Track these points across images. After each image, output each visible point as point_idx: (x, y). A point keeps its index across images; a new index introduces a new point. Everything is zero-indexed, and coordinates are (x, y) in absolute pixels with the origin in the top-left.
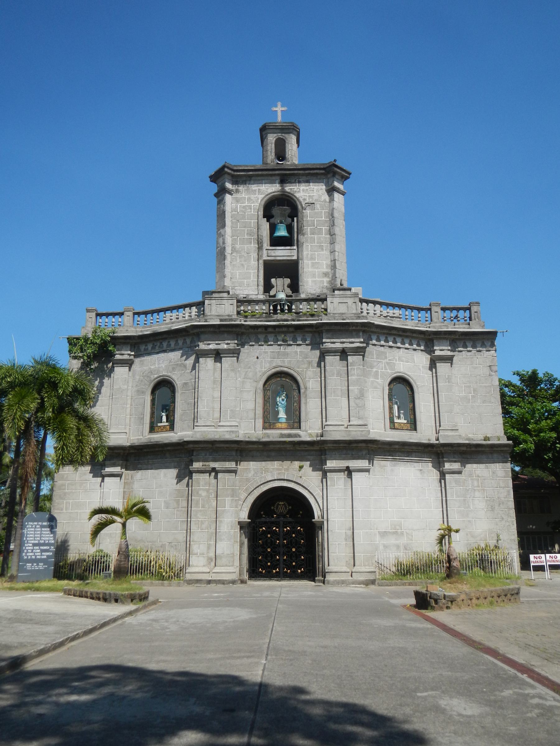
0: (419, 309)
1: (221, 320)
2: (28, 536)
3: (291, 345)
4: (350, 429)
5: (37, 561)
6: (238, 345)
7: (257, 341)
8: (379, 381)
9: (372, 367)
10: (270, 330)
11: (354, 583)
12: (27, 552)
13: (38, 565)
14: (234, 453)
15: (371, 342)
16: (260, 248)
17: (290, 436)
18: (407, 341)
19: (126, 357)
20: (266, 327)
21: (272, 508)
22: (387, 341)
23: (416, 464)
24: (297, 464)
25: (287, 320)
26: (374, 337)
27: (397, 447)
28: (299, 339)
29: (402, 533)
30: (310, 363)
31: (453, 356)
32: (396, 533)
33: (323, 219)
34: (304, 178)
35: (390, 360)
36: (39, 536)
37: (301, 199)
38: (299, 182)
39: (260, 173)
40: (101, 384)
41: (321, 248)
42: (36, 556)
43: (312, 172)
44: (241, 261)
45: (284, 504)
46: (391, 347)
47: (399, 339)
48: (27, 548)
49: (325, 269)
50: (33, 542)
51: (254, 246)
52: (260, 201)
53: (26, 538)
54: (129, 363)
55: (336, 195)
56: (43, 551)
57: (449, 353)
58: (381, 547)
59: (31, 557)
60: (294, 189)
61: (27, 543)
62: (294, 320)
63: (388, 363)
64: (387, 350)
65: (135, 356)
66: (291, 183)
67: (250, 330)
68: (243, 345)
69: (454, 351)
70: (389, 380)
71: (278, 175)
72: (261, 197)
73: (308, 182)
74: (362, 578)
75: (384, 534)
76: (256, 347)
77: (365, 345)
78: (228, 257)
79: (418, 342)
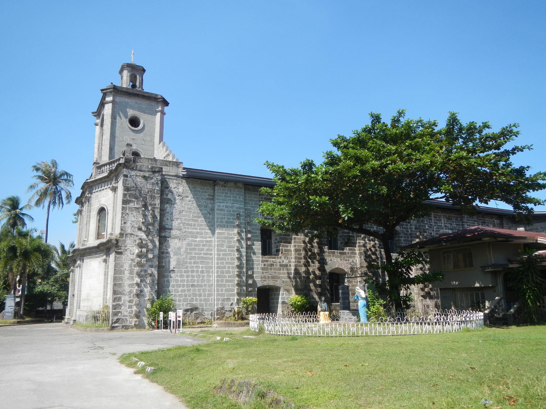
15: (93, 192)
46: (100, 191)
47: (103, 185)
63: (98, 201)
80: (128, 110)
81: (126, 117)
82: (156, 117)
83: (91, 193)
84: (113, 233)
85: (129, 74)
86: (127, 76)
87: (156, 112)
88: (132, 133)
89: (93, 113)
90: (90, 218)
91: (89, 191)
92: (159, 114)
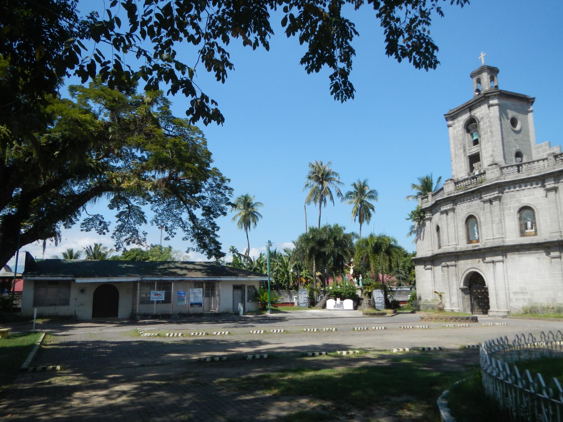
0: (543, 160)
1: (448, 195)
3: (472, 201)
4: (495, 240)
5: (379, 303)
6: (453, 205)
7: (460, 202)
8: (512, 211)
9: (507, 205)
10: (463, 196)
11: (499, 316)
14: (454, 257)
15: (505, 191)
16: (464, 151)
17: (476, 246)
18: (529, 184)
19: (429, 217)
20: (461, 195)
22: (515, 188)
23: (534, 255)
24: (477, 260)
25: (471, 188)
26: (507, 188)
27: (518, 247)
28: (475, 197)
29: (527, 293)
30: (481, 208)
32: (523, 293)
34: (478, 104)
37: (478, 117)
38: (477, 108)
39: (459, 111)
40: (424, 229)
41: (488, 141)
43: (479, 100)
47: (523, 185)
49: (491, 153)
51: (462, 150)
54: (430, 219)
55: (491, 108)
56: (380, 300)
57: (553, 185)
58: (514, 300)
62: (474, 187)
63: (517, 200)
64: (516, 193)
65: (432, 215)
66: (473, 109)
67: (456, 198)
68: (456, 205)
69: (558, 183)
70: (517, 209)
71: (467, 108)
73: (480, 106)
74: (502, 314)
75: (515, 293)
76: (461, 205)
77: (500, 195)
78: (453, 160)
79: (537, 182)
80: (508, 111)
81: (508, 119)
82: (527, 118)
83: (503, 193)
84: (561, 230)
85: (489, 76)
86: (488, 78)
87: (527, 112)
88: (514, 134)
89: (445, 115)
90: (504, 216)
91: (499, 191)
92: (530, 115)
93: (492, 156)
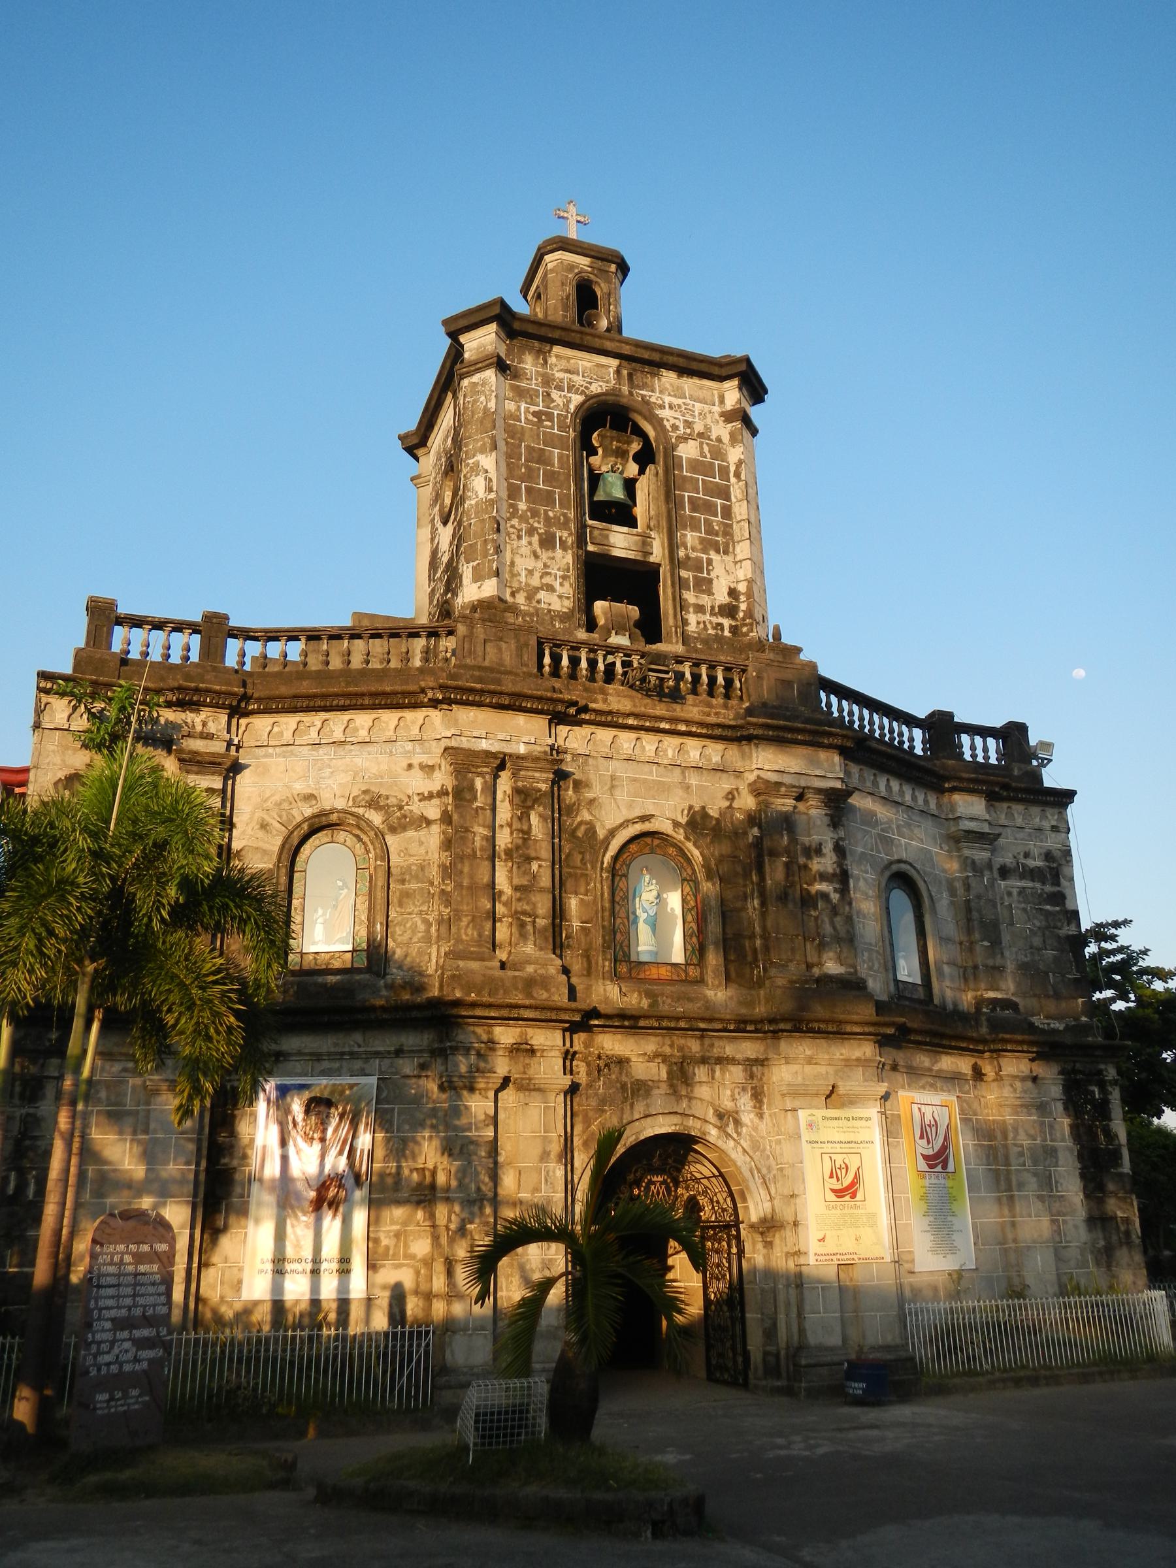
2: (103, 1292)
12: (99, 1353)
13: (126, 1396)
21: (636, 1192)
31: (999, 835)
33: (717, 480)
35: (882, 830)
36: (129, 1290)
42: (121, 1365)
44: (530, 543)
45: (664, 1182)
48: (98, 1337)
50: (113, 1313)
52: (572, 407)
53: (96, 1303)
56: (141, 1344)
59: (108, 1370)
60: (650, 396)
61: (99, 1319)
72: (577, 399)
93: (729, 611)
